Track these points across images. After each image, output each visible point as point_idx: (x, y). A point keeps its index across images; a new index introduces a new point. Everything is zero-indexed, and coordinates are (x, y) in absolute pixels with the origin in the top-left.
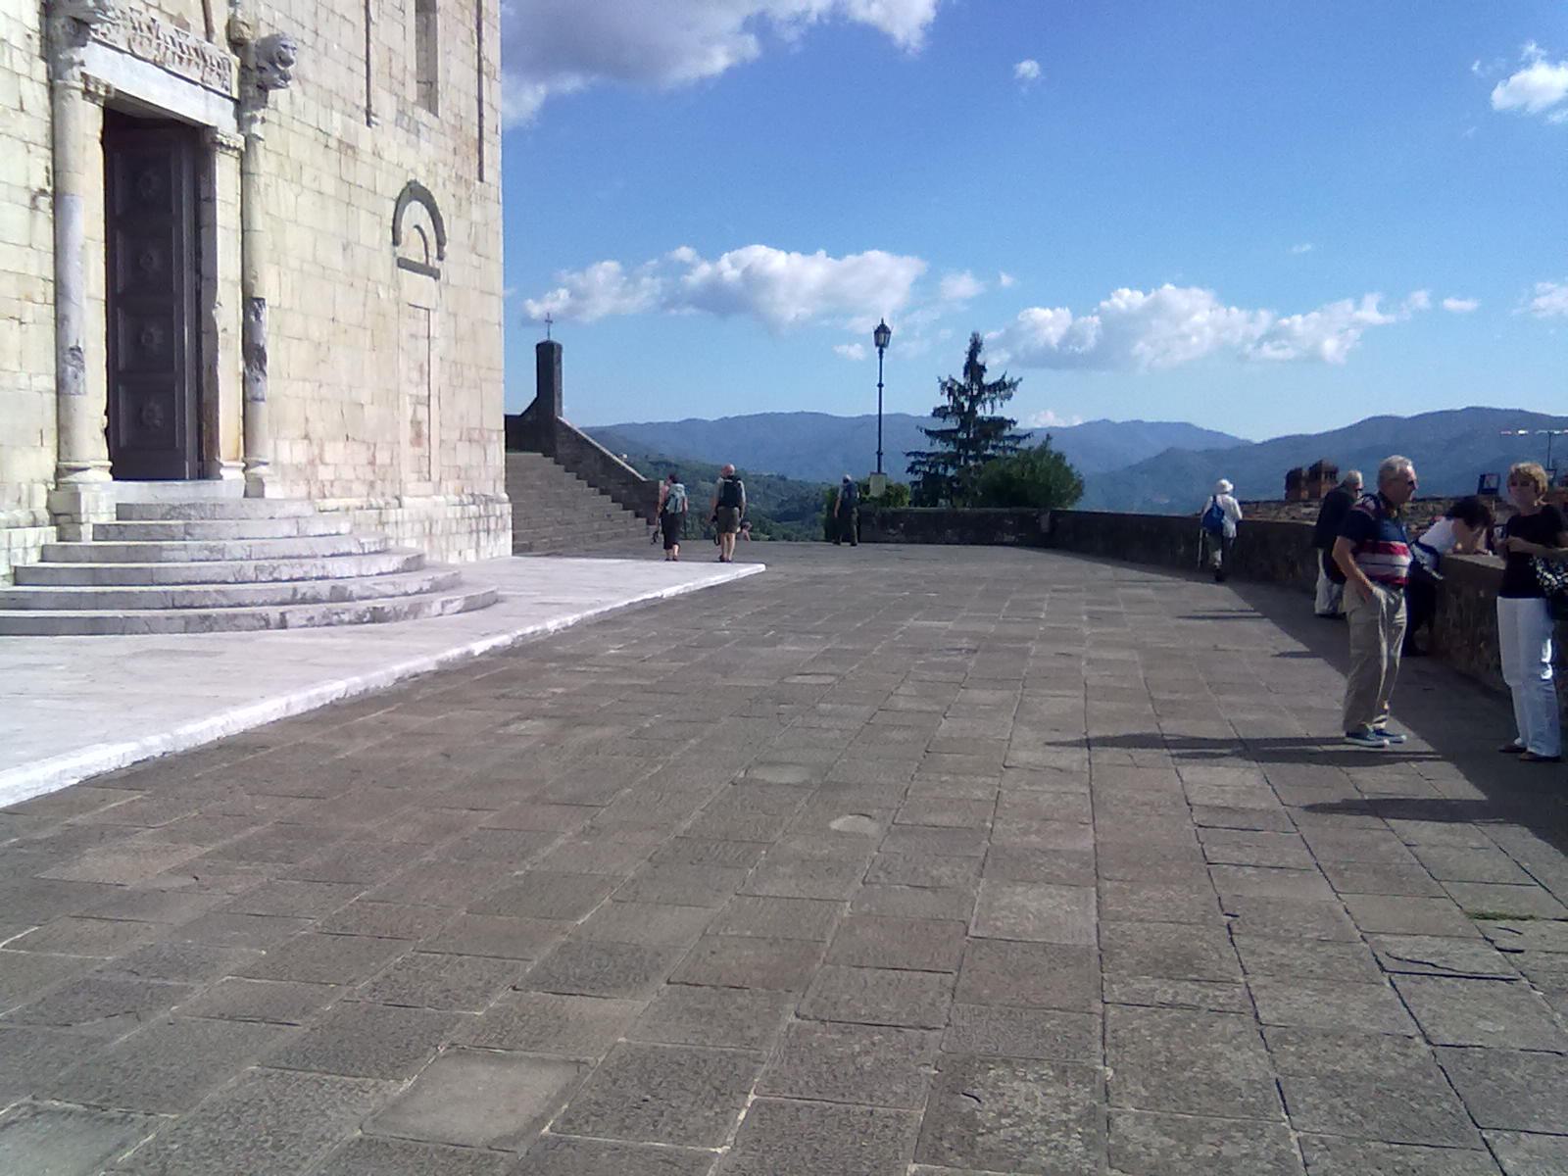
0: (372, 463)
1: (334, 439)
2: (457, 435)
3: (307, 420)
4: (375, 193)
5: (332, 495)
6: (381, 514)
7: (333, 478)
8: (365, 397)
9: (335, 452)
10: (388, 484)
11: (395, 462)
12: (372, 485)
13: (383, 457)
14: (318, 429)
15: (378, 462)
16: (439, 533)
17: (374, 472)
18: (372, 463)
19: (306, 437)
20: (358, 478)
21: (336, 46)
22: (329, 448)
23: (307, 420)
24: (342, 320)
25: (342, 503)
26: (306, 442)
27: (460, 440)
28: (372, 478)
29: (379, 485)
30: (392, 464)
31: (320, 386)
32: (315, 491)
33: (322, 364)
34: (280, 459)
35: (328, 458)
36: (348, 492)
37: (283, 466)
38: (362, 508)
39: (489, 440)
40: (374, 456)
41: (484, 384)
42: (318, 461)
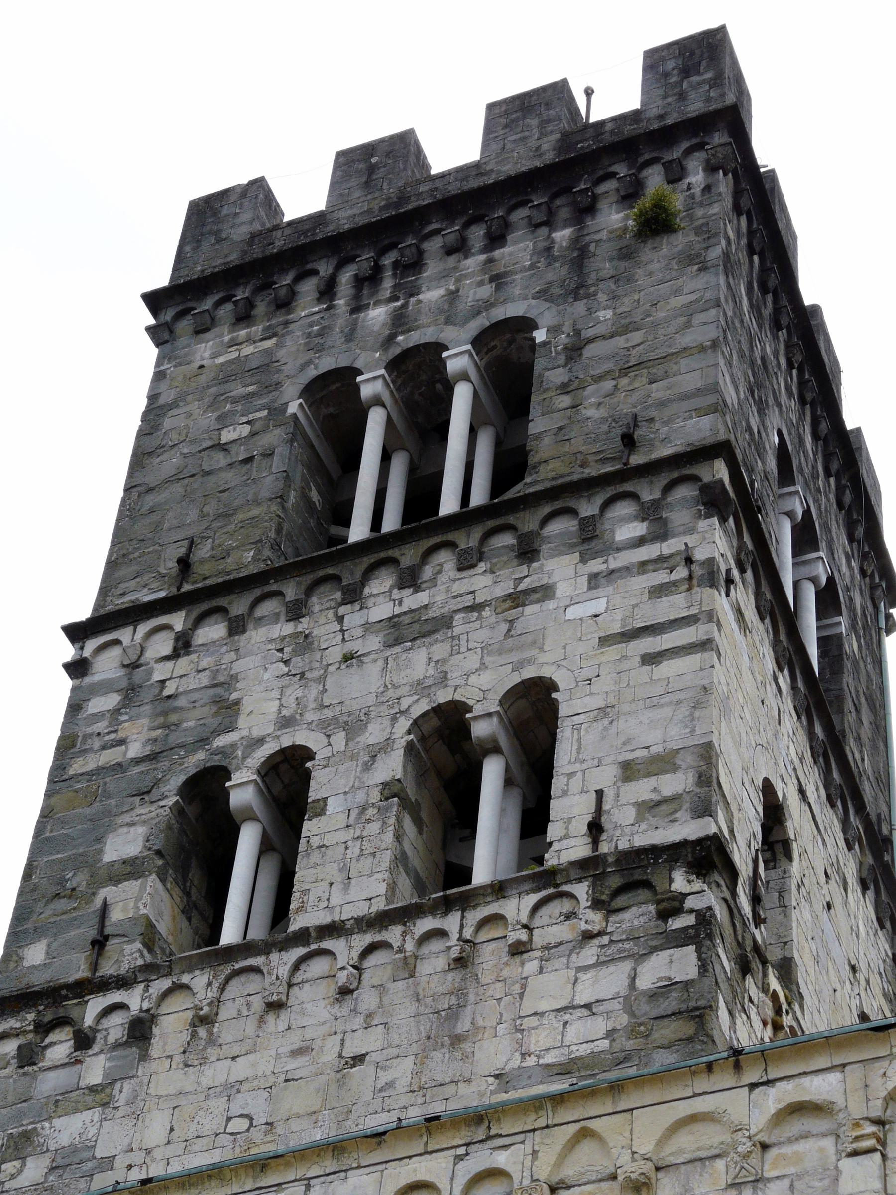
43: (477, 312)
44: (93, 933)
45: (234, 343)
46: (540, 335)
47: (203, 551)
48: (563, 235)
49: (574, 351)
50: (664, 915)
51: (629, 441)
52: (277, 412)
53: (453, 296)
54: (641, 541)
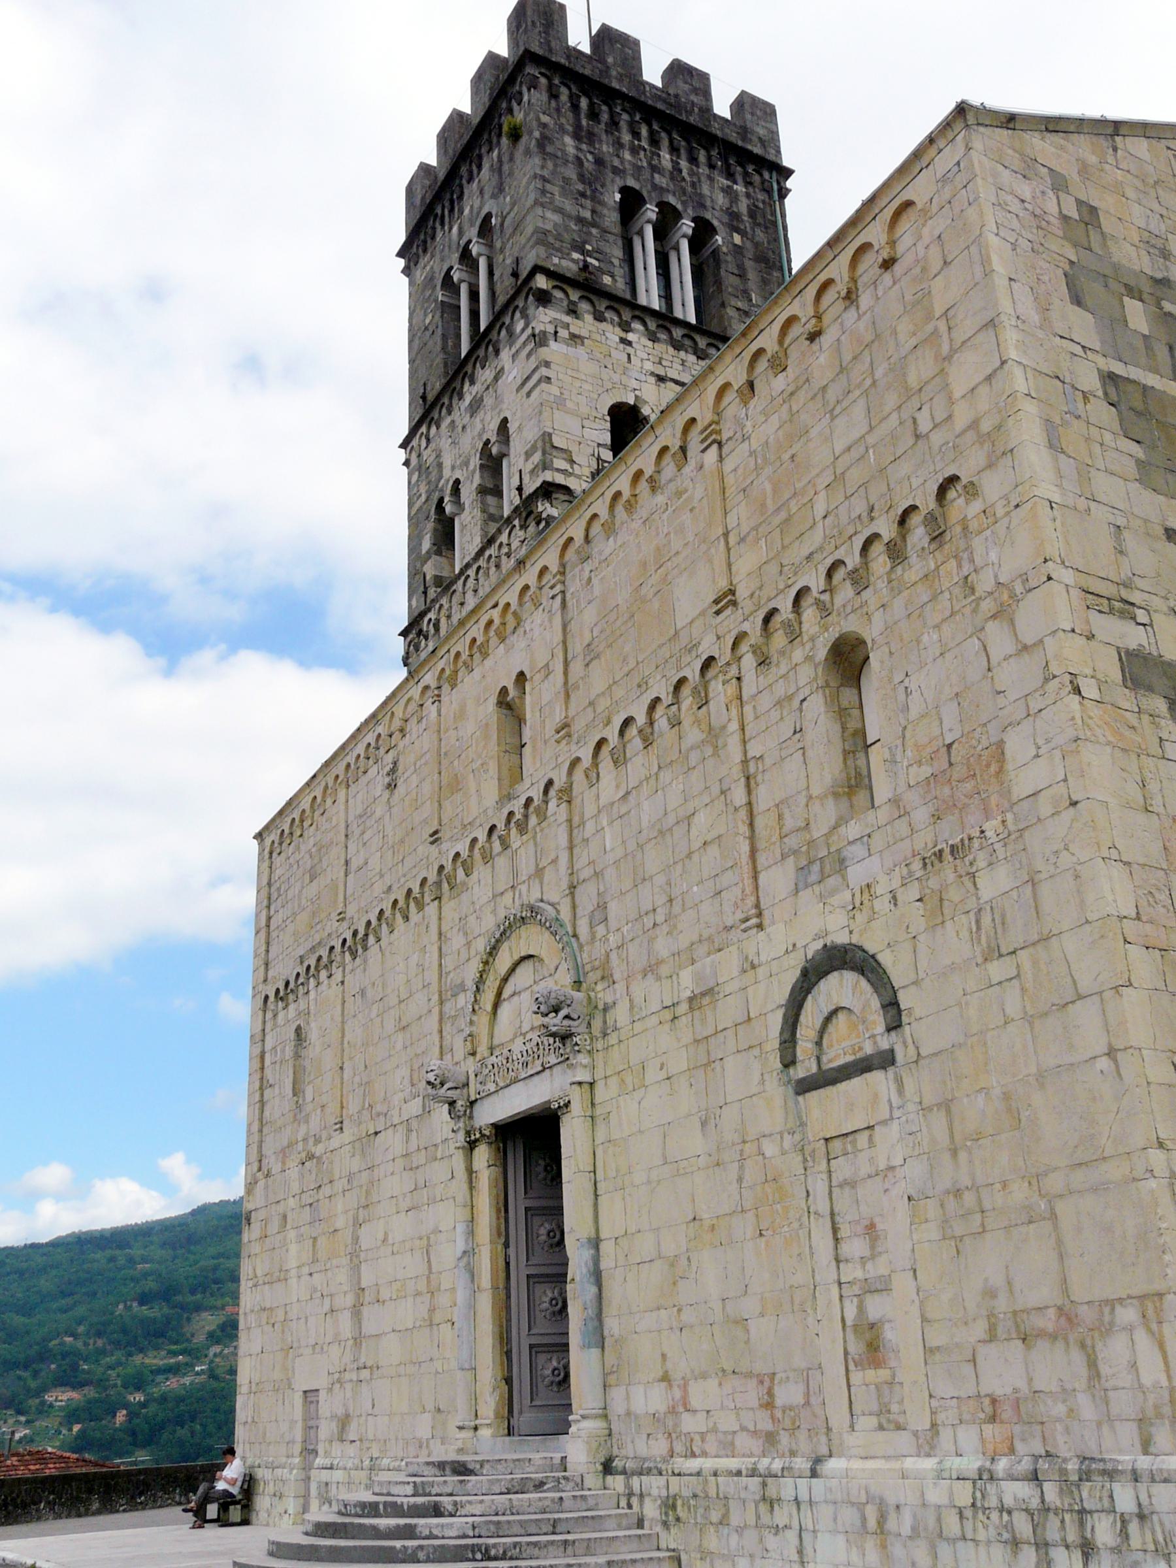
0: (769, 1404)
1: (704, 1376)
2: (980, 1329)
3: (664, 1356)
4: (749, 1019)
5: (704, 1454)
6: (764, 1485)
7: (704, 1430)
8: (749, 1307)
9: (704, 1394)
10: (802, 1435)
11: (813, 1400)
12: (770, 1438)
13: (789, 1394)
14: (679, 1368)
15: (779, 1402)
16: (906, 1530)
17: (772, 1417)
18: (769, 1405)
19: (665, 1378)
20: (743, 1429)
21: (695, 889)
22: (695, 1389)
23: (664, 1356)
24: (705, 1216)
25: (707, 1464)
26: (664, 1384)
27: (992, 1336)
28: (768, 1426)
29: (784, 1439)
30: (807, 1403)
31: (679, 1310)
32: (679, 1448)
33: (681, 1283)
34: (633, 1409)
35: (695, 1402)
36: (729, 1449)
37: (637, 1417)
38: (739, 1473)
39: (1106, 1330)
40: (770, 1393)
41: (1060, 1207)
42: (681, 1409)
43: (478, 213)
44: (422, 589)
45: (425, 266)
46: (493, 221)
47: (428, 388)
48: (496, 153)
49: (502, 225)
50: (538, 523)
51: (515, 274)
52: (436, 301)
53: (472, 207)
54: (523, 330)
